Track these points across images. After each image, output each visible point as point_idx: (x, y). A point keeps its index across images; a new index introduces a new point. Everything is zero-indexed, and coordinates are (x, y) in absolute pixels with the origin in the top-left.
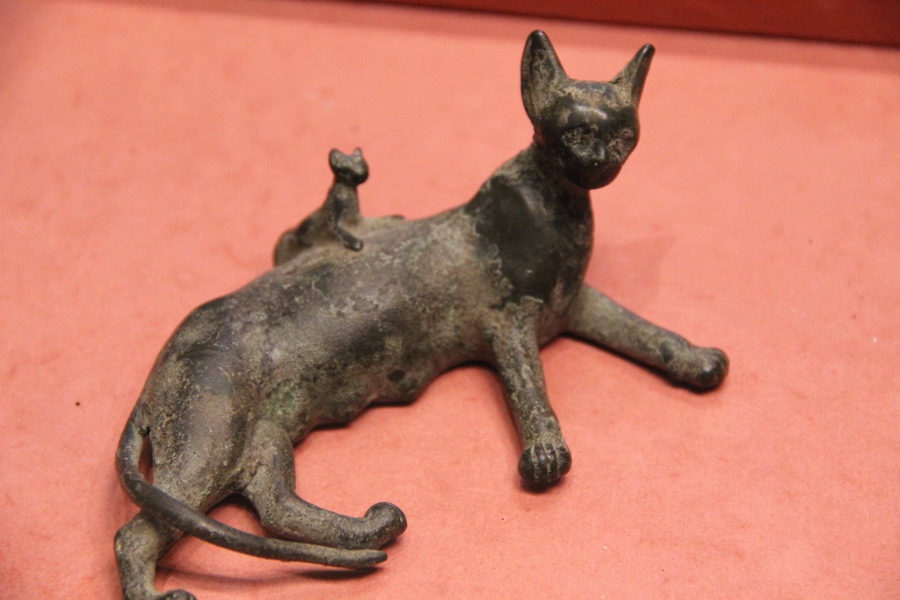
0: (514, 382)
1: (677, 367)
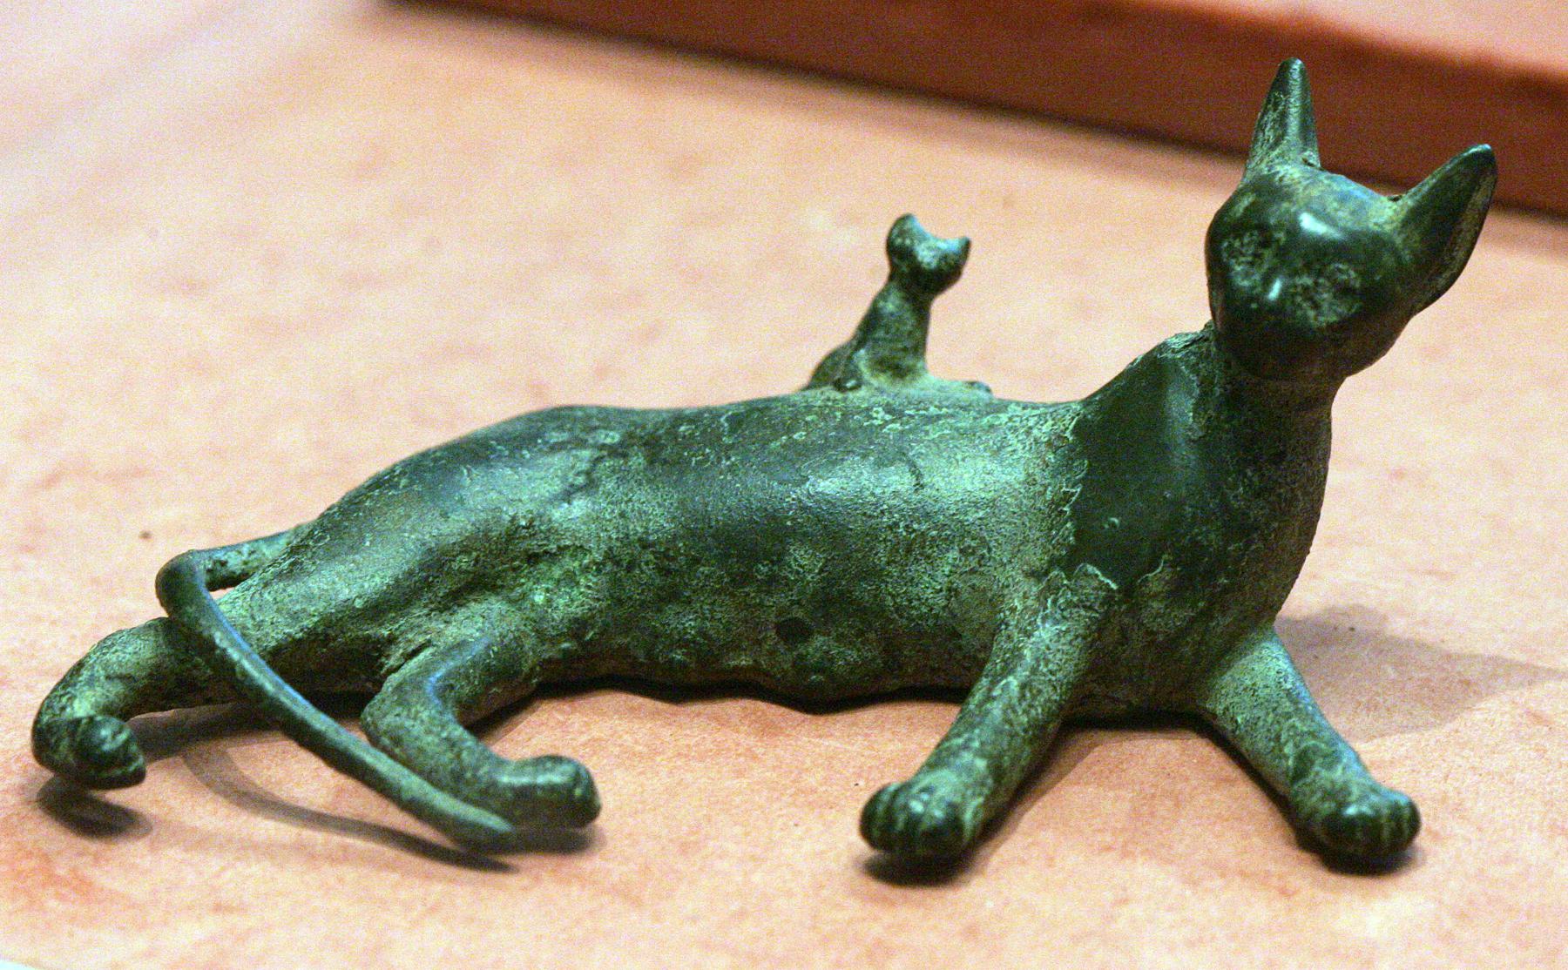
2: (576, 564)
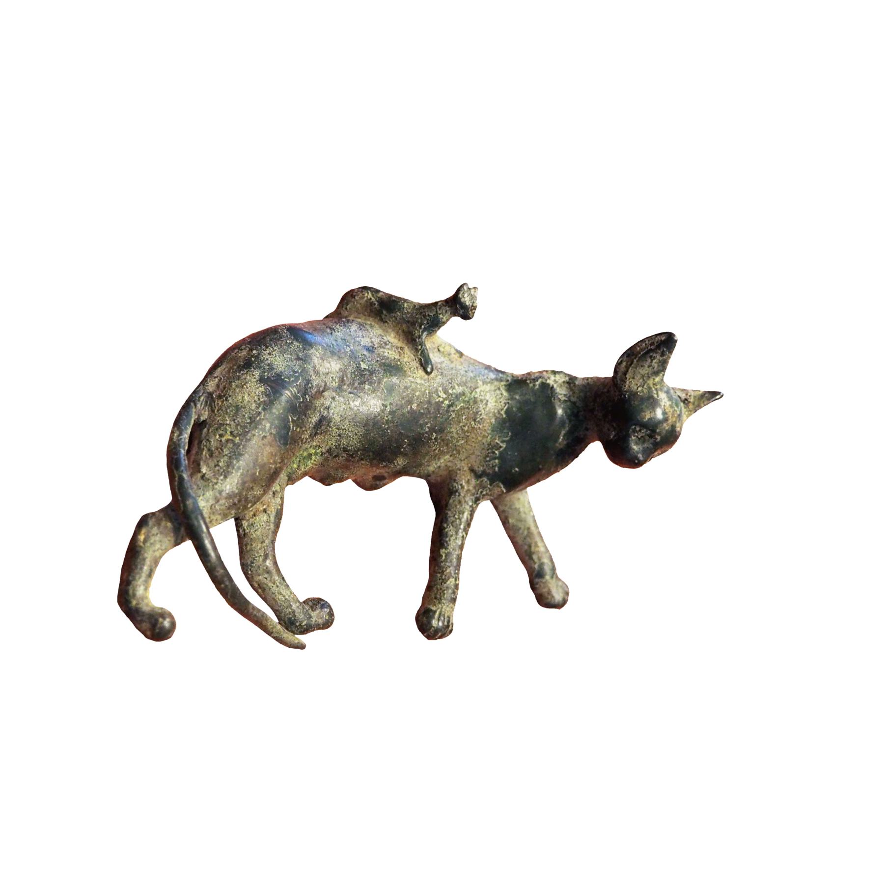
0: (450, 540)
1: (540, 586)
2: (314, 451)
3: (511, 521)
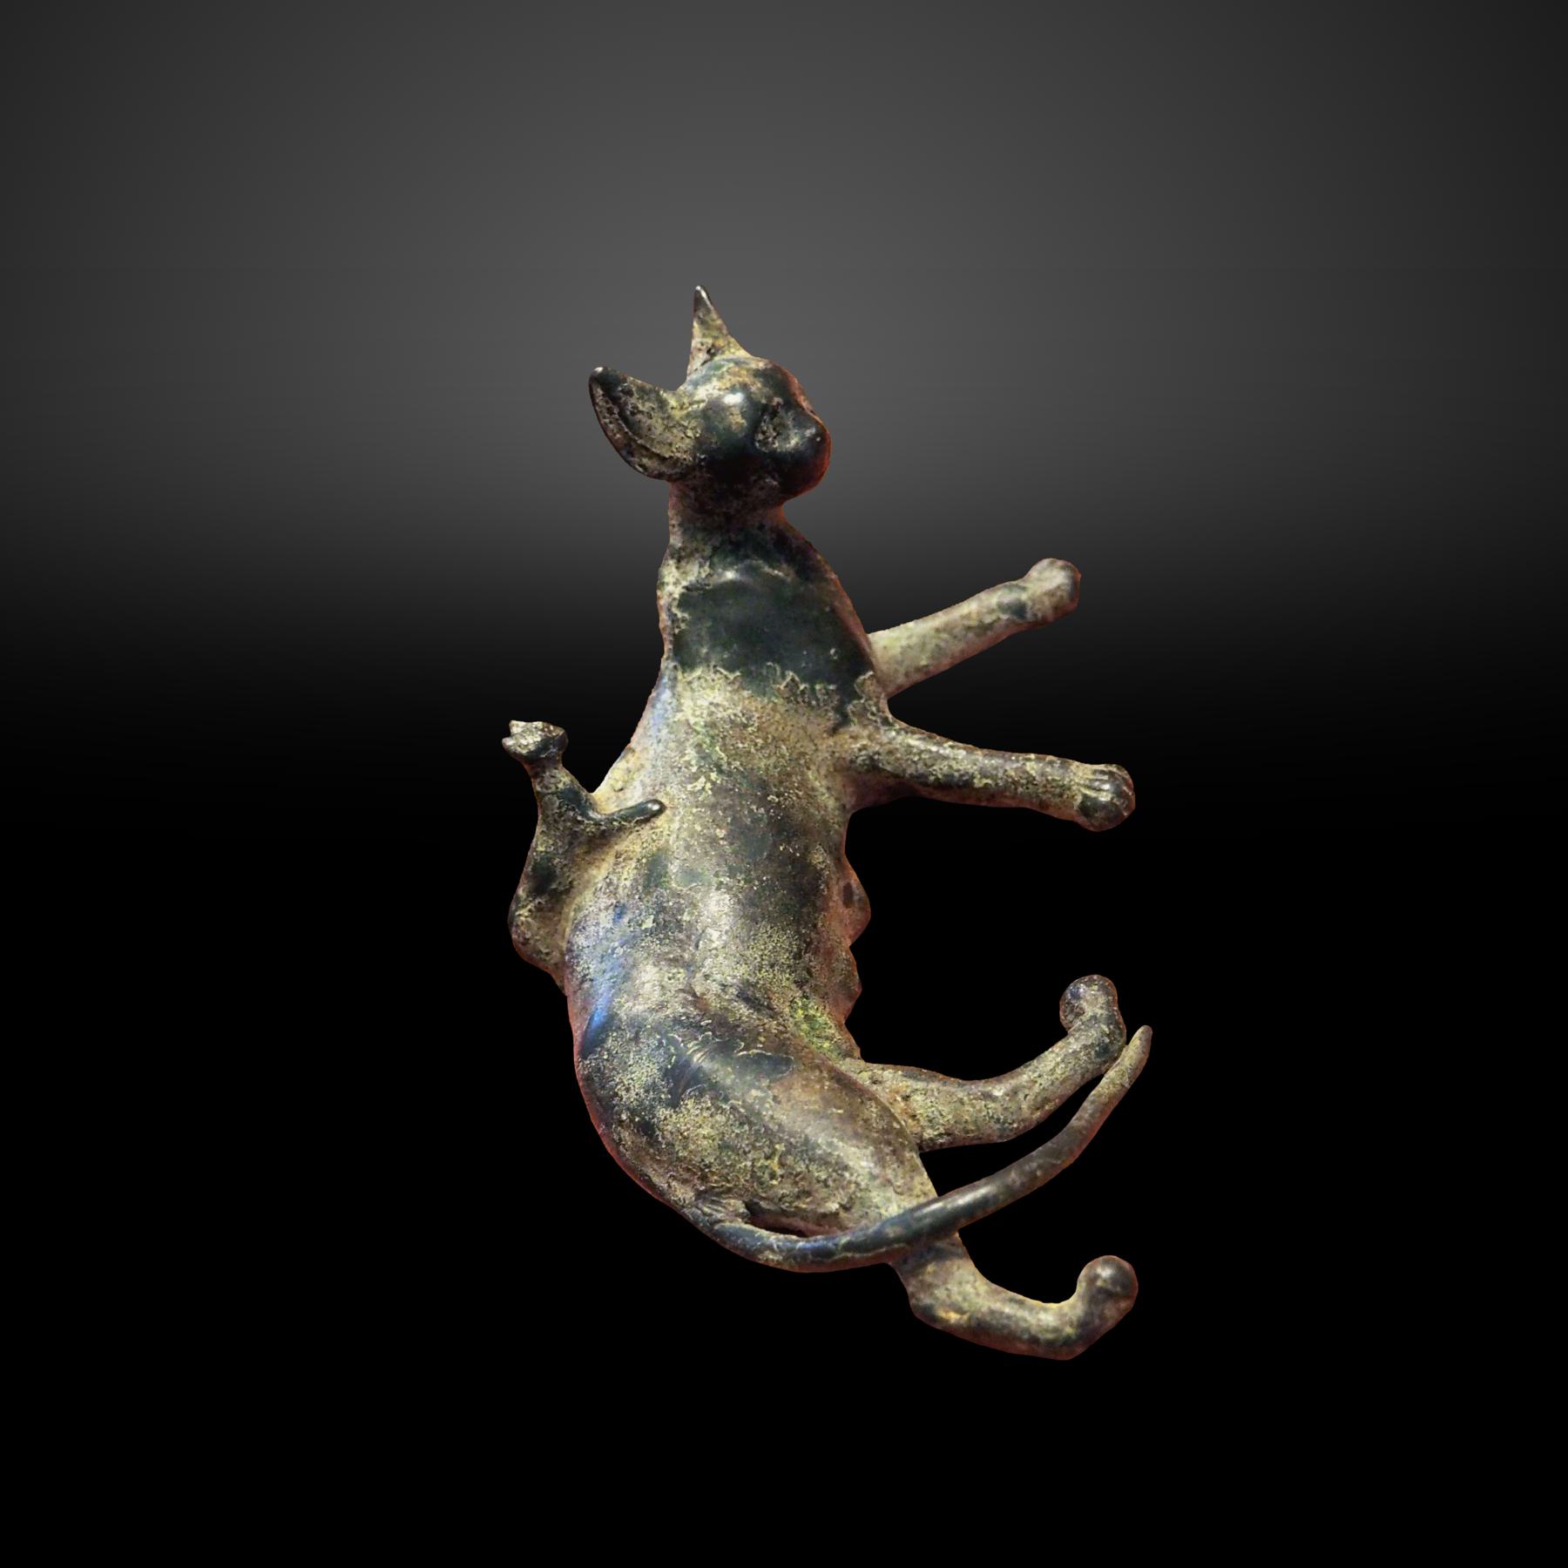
0: (958, 771)
1: (1039, 609)
2: (800, 1012)
3: (924, 662)
